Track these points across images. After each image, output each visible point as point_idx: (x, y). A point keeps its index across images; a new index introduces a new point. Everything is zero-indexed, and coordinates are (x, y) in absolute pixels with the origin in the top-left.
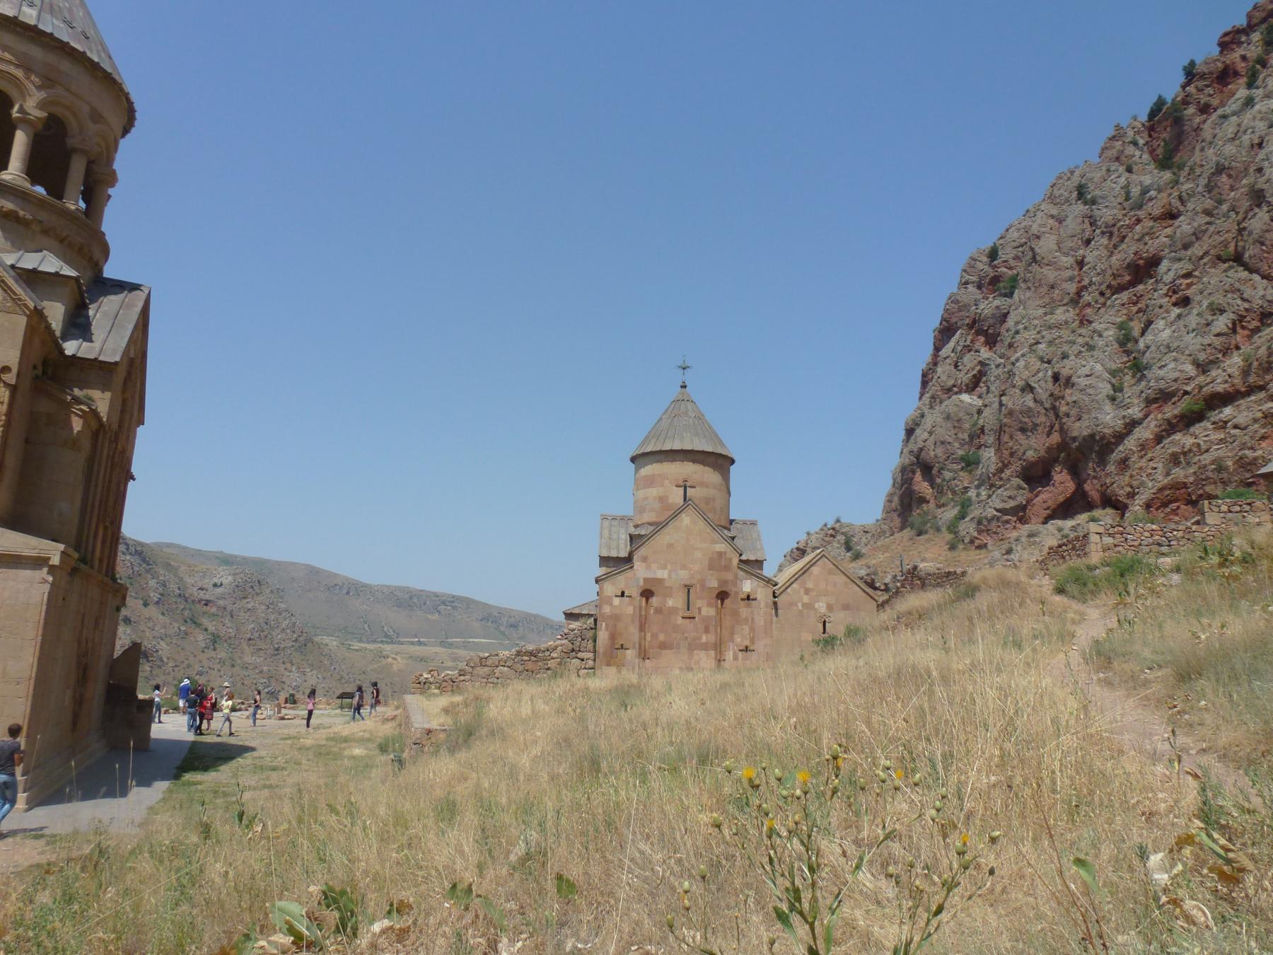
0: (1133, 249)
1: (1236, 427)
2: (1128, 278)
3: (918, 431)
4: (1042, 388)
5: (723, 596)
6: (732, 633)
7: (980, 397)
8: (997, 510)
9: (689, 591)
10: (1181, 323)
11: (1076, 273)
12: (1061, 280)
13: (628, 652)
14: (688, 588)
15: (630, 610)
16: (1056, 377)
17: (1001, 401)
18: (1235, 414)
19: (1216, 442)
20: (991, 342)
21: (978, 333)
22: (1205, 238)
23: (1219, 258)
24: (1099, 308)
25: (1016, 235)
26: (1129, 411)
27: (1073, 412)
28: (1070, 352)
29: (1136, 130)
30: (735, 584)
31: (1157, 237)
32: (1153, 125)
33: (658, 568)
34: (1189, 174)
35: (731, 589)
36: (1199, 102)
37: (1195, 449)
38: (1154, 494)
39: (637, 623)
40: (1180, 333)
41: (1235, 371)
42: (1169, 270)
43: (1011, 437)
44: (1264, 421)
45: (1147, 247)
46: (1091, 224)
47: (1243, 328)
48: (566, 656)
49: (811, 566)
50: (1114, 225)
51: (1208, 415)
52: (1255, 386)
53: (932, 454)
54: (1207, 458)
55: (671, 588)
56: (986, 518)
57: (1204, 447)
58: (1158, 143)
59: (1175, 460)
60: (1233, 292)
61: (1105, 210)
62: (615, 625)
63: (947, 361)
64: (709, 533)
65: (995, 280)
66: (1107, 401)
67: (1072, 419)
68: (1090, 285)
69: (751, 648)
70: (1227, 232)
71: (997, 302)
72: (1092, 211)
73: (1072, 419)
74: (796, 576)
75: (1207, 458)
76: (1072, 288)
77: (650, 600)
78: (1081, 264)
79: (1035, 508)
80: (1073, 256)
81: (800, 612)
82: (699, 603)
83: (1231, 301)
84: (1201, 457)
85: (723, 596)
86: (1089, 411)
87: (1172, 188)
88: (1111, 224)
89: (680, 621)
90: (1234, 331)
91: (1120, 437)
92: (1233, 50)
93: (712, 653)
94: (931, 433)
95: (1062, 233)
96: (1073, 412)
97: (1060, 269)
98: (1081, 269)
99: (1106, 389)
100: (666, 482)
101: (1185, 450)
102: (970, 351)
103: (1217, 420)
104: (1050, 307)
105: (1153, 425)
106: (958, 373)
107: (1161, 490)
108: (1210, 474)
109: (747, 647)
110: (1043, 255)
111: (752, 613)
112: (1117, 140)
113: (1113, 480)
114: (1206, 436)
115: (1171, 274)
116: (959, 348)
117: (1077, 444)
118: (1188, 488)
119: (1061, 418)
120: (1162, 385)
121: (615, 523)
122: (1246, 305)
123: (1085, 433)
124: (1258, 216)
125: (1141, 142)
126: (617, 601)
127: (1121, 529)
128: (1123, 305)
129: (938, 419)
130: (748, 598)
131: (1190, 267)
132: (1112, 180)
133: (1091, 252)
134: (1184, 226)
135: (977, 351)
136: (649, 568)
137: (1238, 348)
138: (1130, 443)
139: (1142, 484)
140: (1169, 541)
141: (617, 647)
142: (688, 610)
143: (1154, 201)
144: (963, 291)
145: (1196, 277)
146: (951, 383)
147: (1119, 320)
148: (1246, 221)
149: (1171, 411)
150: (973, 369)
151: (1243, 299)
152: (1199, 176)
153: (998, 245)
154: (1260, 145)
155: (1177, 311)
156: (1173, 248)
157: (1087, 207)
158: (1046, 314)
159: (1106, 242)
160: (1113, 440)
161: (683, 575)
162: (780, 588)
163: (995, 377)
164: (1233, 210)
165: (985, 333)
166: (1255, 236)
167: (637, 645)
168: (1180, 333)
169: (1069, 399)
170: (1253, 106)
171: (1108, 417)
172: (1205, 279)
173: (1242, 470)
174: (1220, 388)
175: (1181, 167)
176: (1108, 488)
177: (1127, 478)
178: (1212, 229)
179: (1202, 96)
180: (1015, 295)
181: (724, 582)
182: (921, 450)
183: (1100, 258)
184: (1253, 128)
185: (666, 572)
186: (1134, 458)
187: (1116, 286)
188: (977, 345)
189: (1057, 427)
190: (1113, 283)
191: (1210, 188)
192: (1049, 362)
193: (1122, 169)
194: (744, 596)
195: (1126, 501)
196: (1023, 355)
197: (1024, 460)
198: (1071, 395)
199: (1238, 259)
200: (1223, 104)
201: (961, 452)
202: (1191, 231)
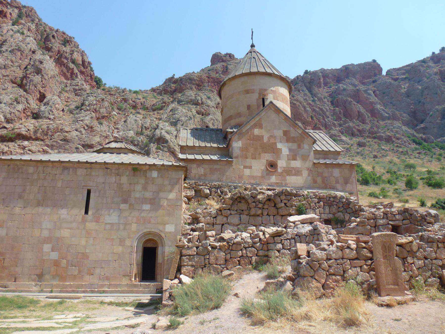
1: (29, 150)
18: (30, 145)
22: (9, 70)
37: (9, 153)
47: (24, 113)
51: (17, 141)
52: (39, 138)
70: (17, 73)
92: (4, 7)
101: (4, 151)
114: (14, 149)
122: (29, 106)
151: (28, 103)
154: (34, 52)
174: (24, 133)
178: (12, 69)
202: (4, 64)
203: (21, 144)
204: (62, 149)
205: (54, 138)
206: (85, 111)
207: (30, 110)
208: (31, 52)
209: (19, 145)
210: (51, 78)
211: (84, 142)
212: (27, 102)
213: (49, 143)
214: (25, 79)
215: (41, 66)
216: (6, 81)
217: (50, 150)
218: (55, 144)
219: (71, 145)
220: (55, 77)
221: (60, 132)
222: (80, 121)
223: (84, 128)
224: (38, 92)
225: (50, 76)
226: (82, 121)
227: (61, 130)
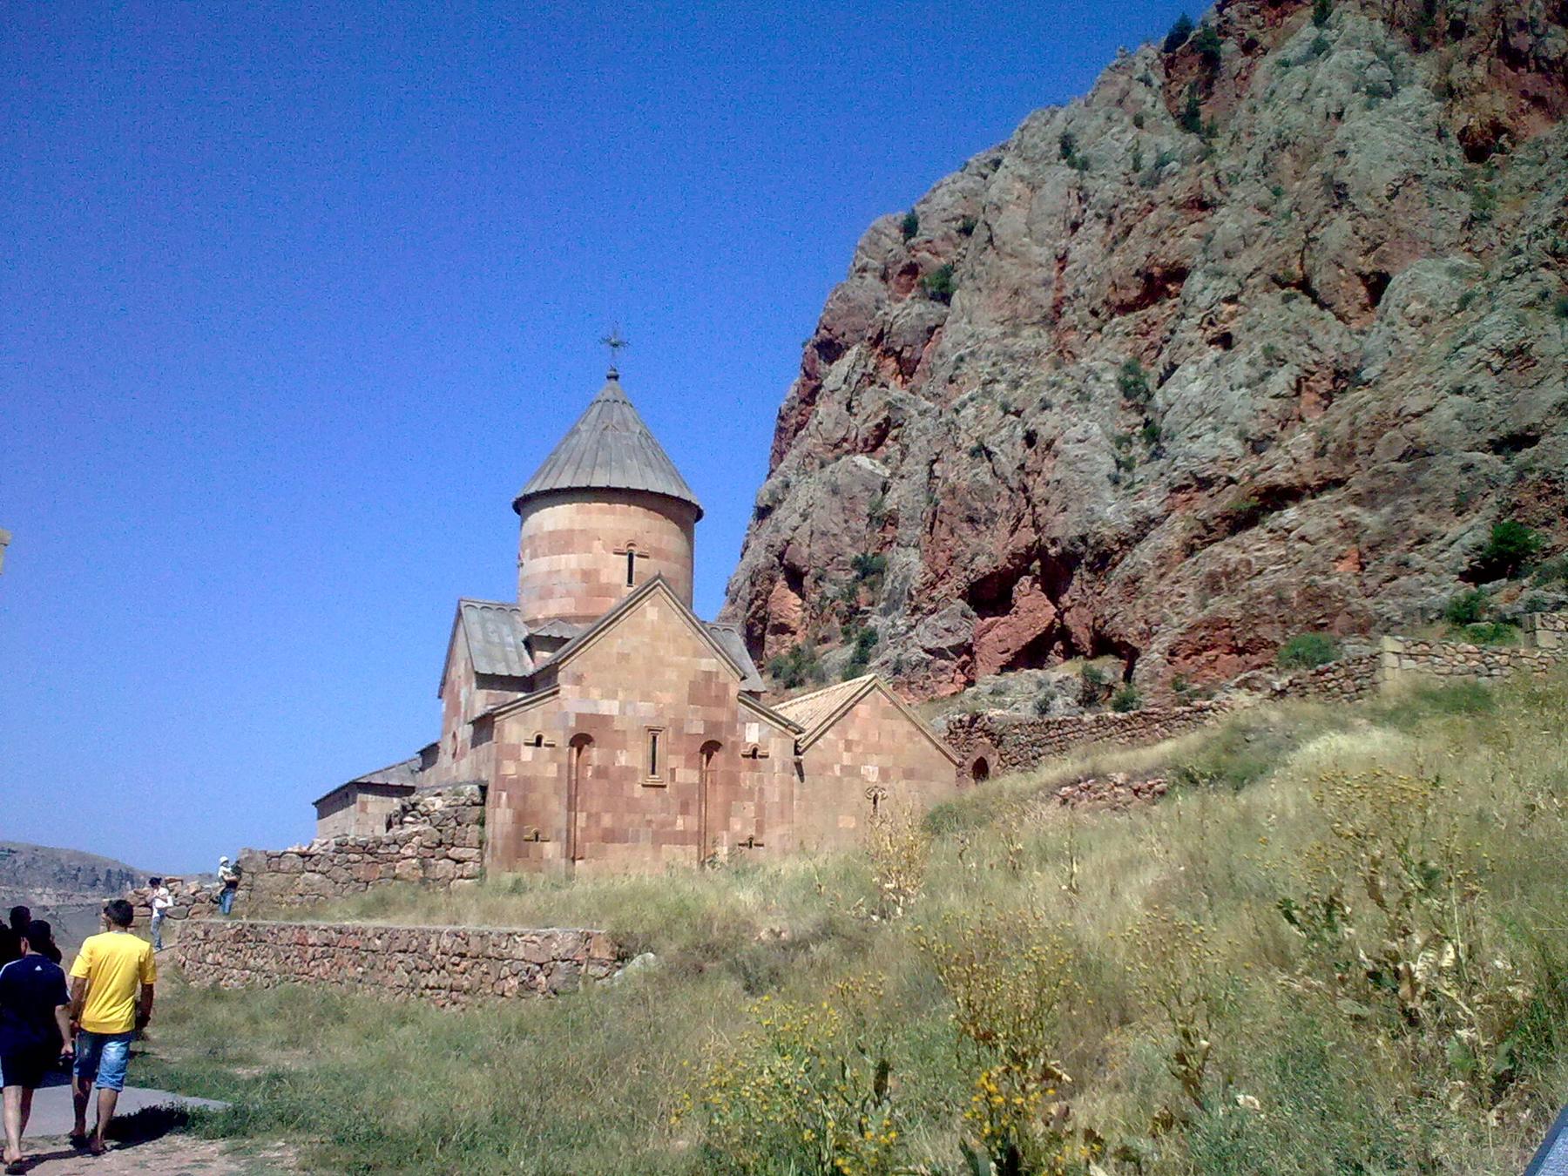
0: (1144, 249)
1: (1302, 538)
2: (1135, 293)
3: (779, 513)
4: (1007, 456)
5: (710, 748)
6: (727, 816)
7: (885, 461)
8: (928, 651)
9: (654, 738)
10: (1222, 373)
11: (1054, 274)
12: (1030, 282)
13: (547, 845)
14: (654, 733)
15: (551, 771)
16: (1030, 439)
17: (932, 471)
19: (1273, 560)
20: (907, 369)
21: (887, 353)
23: (1275, 279)
24: (1089, 336)
25: (947, 200)
26: (1144, 503)
27: (1056, 498)
28: (1054, 401)
29: (1148, 61)
30: (732, 729)
31: (1181, 235)
32: (1174, 58)
33: (603, 697)
34: (1231, 144)
35: (727, 739)
36: (1243, 35)
38: (1182, 634)
39: (565, 794)
40: (1220, 388)
41: (1304, 455)
42: (1205, 288)
43: (952, 532)
44: (1342, 533)
45: (1165, 248)
46: (1080, 199)
47: (1309, 389)
48: (429, 853)
49: (857, 702)
50: (1115, 206)
52: (1330, 480)
53: (805, 551)
54: (1260, 585)
55: (624, 732)
56: (909, 663)
57: (1256, 568)
58: (1178, 89)
59: (1213, 584)
60: (1297, 334)
61: (1102, 181)
62: (524, 798)
63: (837, 396)
64: (689, 638)
65: (912, 270)
66: (1108, 484)
67: (1054, 508)
68: (1076, 297)
69: (760, 841)
71: (919, 308)
72: (1082, 178)
73: (1054, 508)
74: (833, 719)
75: (1260, 585)
76: (1047, 298)
77: (584, 754)
78: (1062, 260)
79: (986, 651)
80: (1050, 247)
81: (839, 779)
82: (673, 761)
83: (1294, 347)
84: (1253, 582)
85: (710, 748)
86: (1080, 499)
87: (1200, 161)
88: (1111, 202)
89: (638, 791)
90: (1298, 392)
91: (1127, 543)
93: (694, 849)
94: (804, 517)
95: (1035, 206)
96: (1056, 498)
97: (1030, 265)
98: (1062, 269)
99: (1108, 465)
100: (597, 545)
101: (1229, 569)
102: (872, 383)
103: (1275, 528)
104: (1014, 326)
105: (1178, 527)
106: (851, 419)
107: (1193, 629)
108: (1266, 609)
109: (751, 839)
110: (1004, 239)
111: (760, 779)
112: (1123, 74)
113: (1115, 611)
114: (1259, 550)
115: (1208, 294)
116: (856, 377)
117: (1059, 549)
118: (1232, 628)
119: (1034, 506)
120: (1195, 466)
121: (489, 615)
123: (1074, 532)
124: (1335, 223)
125: (1157, 82)
126: (527, 754)
127: (1426, 648)
128: (1128, 334)
129: (819, 494)
130: (754, 755)
131: (1236, 289)
132: (1113, 135)
133: (1079, 244)
134: (1228, 223)
135: (883, 385)
136: (585, 695)
137: (1301, 419)
138: (1143, 554)
139: (1163, 619)
140: (1490, 669)
141: (526, 836)
142: (653, 772)
143: (1176, 178)
144: (857, 281)
145: (1243, 304)
146: (840, 434)
147: (1122, 358)
148: (1319, 228)
149: (1206, 506)
150: (876, 415)
151: (1313, 348)
152: (1249, 149)
153: (918, 213)
154: (1339, 116)
155: (1215, 352)
156: (1210, 255)
157: (1075, 171)
158: (1004, 334)
159: (1103, 232)
160: (1116, 547)
161: (646, 708)
162: (807, 738)
163: (918, 430)
164: (1296, 209)
165: (898, 356)
166: (1330, 254)
167: (564, 835)
168: (1220, 388)
169: (1049, 476)
170: (1328, 55)
171: (1109, 510)
172: (1255, 309)
173: (1310, 604)
174: (1281, 479)
175: (1211, 132)
176: (1106, 622)
177: (1140, 611)
178: (1267, 233)
179: (1246, 27)
180: (955, 299)
181: (712, 726)
182: (788, 543)
183: (1091, 256)
184: (1329, 88)
185: (616, 704)
186: (1149, 578)
187: (1118, 303)
188: (884, 375)
189: (1027, 520)
190: (1112, 298)
191: (1266, 168)
192: (1018, 413)
193: (1127, 120)
194: (749, 751)
195: (1135, 645)
196: (972, 399)
197: (972, 570)
198: (1053, 470)
199: (1304, 285)
200: (1277, 44)
201: (853, 554)
203: (1275, 525)
204: (1407, 493)
205: (1375, 462)
206: (1511, 279)
207: (1328, 368)
208: (1333, 118)
209: (1271, 531)
210: (1390, 198)
211: (1493, 430)
212: (1310, 345)
213: (1358, 489)
214: (1307, 252)
215: (1342, 176)
216: (1257, 290)
217: (1367, 514)
218: (1379, 482)
219: (1439, 463)
220: (1418, 177)
221: (1395, 425)
222: (1464, 344)
223: (1488, 365)
224: (1358, 280)
225: (1385, 193)
226: (1473, 341)
227: (1397, 415)
